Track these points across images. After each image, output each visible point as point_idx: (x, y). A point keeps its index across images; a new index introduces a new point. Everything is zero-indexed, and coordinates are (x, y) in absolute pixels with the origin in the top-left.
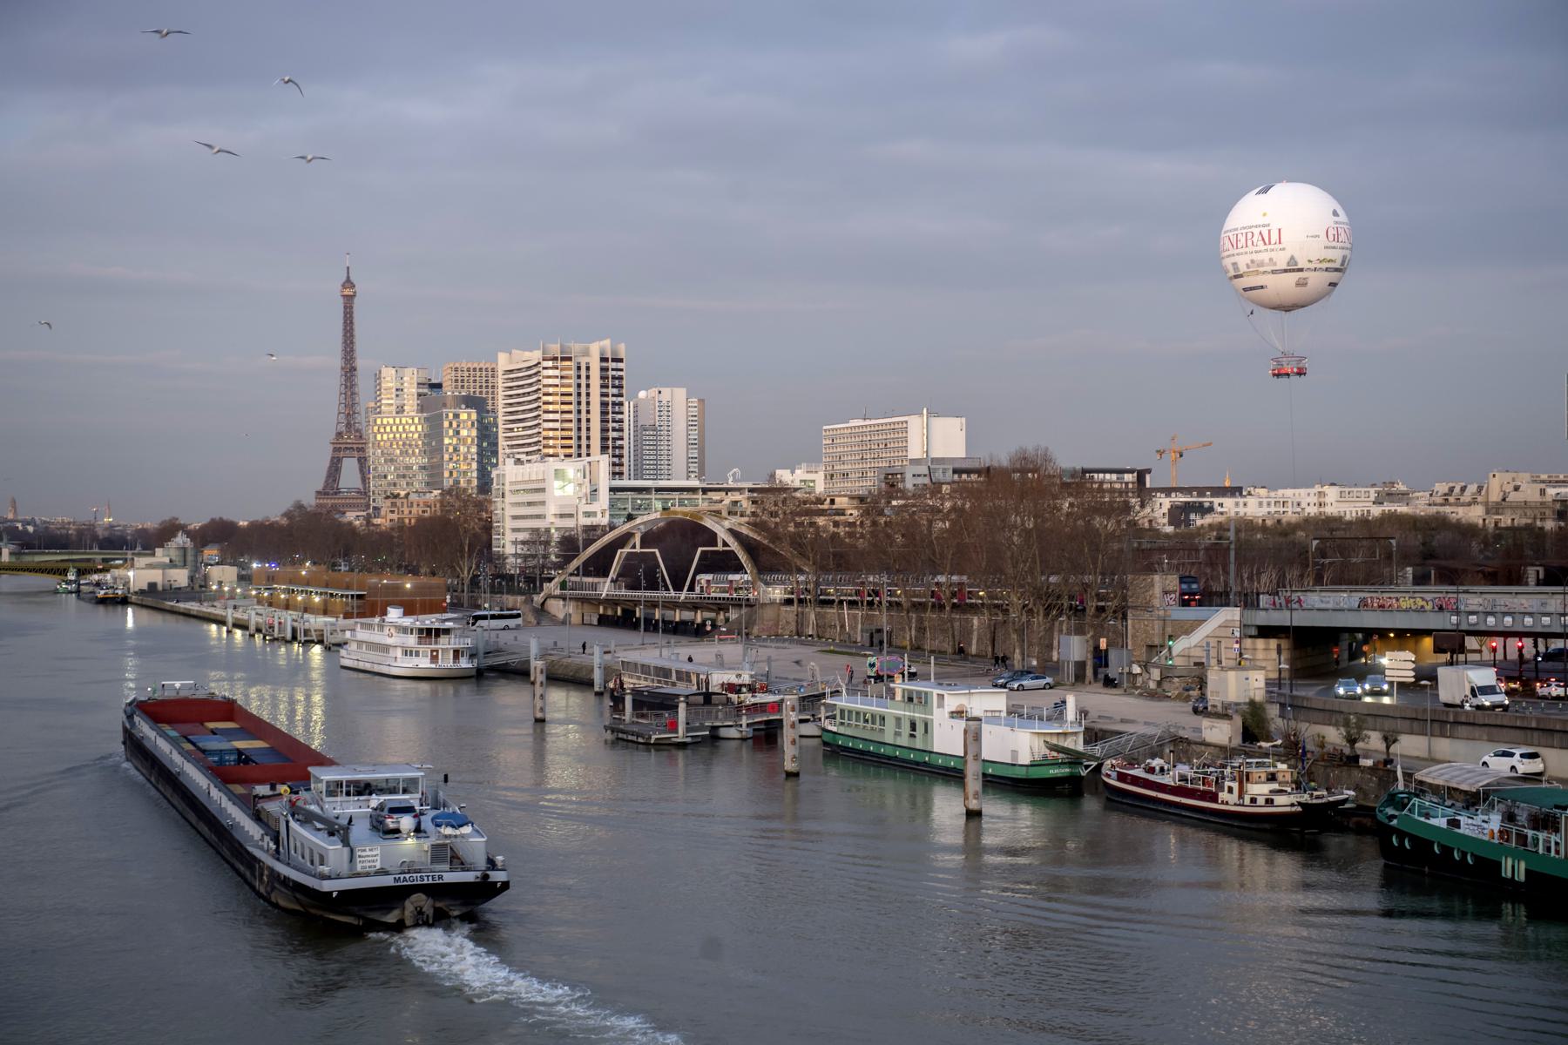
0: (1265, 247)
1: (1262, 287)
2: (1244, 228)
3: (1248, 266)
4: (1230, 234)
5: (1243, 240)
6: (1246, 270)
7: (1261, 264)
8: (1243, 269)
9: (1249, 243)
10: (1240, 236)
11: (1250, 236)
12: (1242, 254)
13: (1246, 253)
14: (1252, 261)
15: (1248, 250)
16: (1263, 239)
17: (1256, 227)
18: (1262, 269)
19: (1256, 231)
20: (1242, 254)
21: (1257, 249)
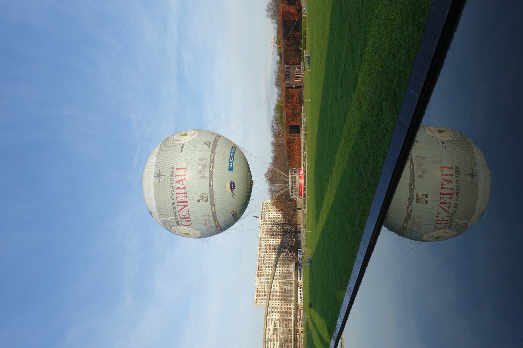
2: (172, 193)
5: (182, 196)
9: (183, 191)
10: (179, 200)
11: (179, 191)
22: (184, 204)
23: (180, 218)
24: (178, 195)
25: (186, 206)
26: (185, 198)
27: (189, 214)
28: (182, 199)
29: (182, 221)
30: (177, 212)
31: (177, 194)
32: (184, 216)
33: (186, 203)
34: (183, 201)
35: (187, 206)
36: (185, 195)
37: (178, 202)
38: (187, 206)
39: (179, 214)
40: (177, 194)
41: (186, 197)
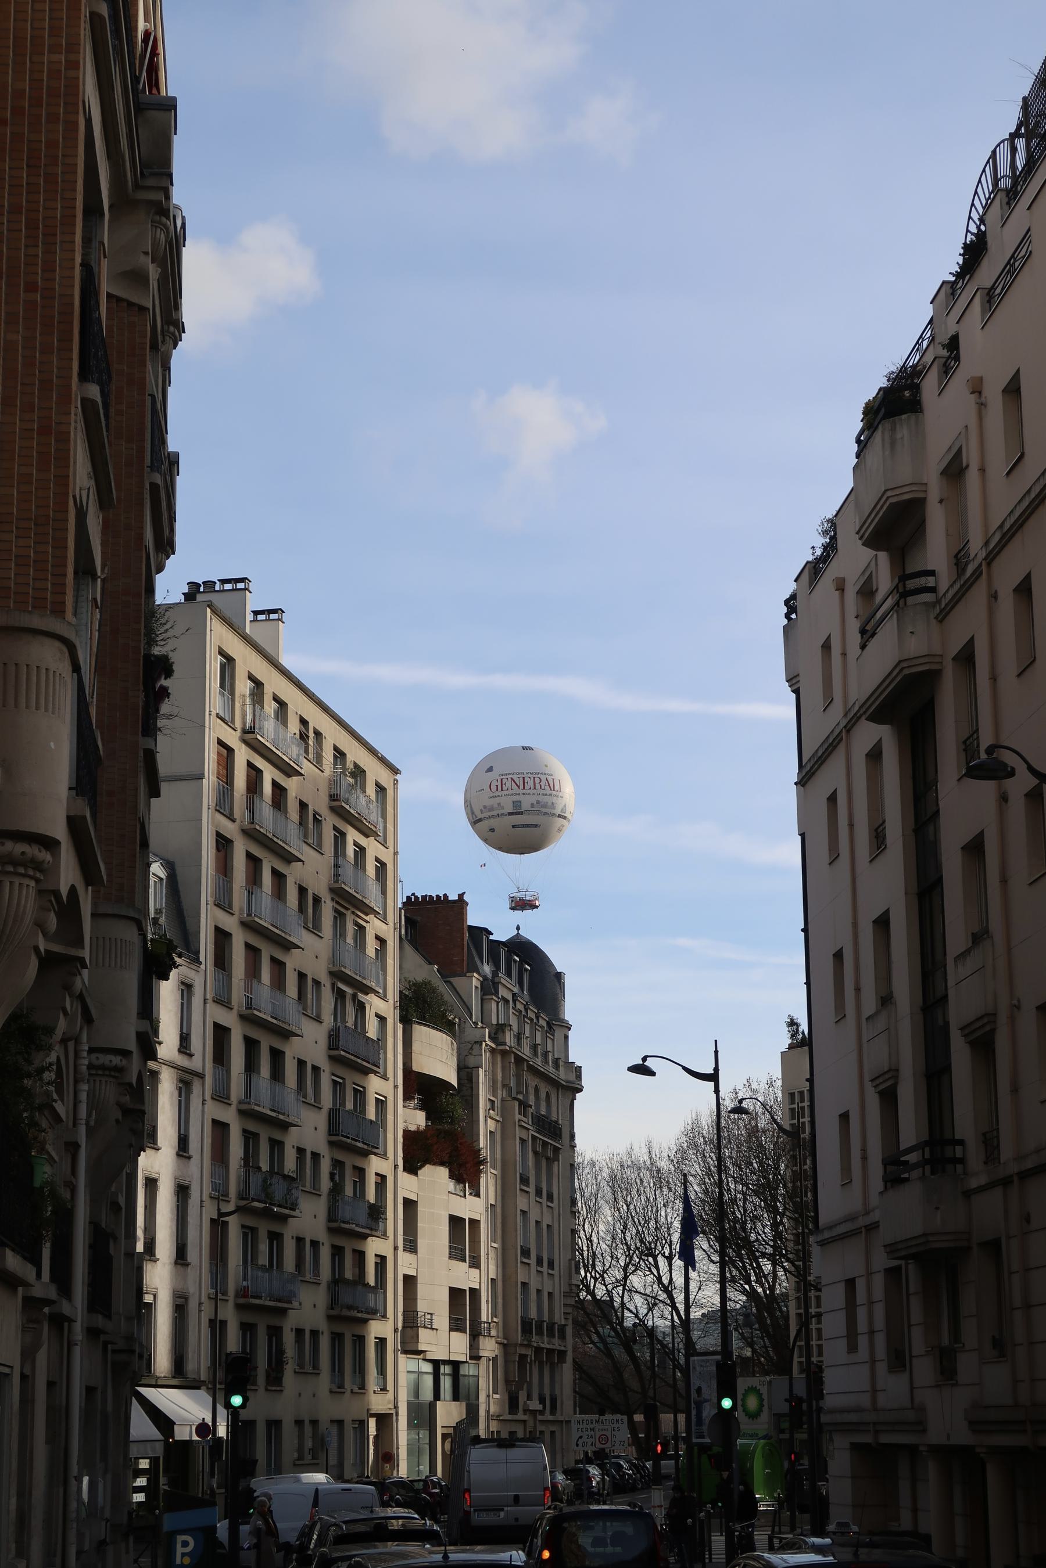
0: (550, 792)
1: (536, 826)
3: (532, 805)
4: (515, 777)
5: (531, 783)
7: (545, 806)
8: (526, 806)
9: (538, 786)
10: (526, 780)
11: (537, 780)
12: (529, 794)
13: (534, 794)
14: (538, 802)
15: (535, 791)
16: (549, 785)
17: (542, 774)
18: (544, 810)
19: (543, 778)
20: (529, 794)
22: (521, 787)
24: (532, 779)
25: (519, 787)
31: (534, 778)
34: (526, 784)
36: (533, 787)
37: (524, 778)
40: (534, 778)
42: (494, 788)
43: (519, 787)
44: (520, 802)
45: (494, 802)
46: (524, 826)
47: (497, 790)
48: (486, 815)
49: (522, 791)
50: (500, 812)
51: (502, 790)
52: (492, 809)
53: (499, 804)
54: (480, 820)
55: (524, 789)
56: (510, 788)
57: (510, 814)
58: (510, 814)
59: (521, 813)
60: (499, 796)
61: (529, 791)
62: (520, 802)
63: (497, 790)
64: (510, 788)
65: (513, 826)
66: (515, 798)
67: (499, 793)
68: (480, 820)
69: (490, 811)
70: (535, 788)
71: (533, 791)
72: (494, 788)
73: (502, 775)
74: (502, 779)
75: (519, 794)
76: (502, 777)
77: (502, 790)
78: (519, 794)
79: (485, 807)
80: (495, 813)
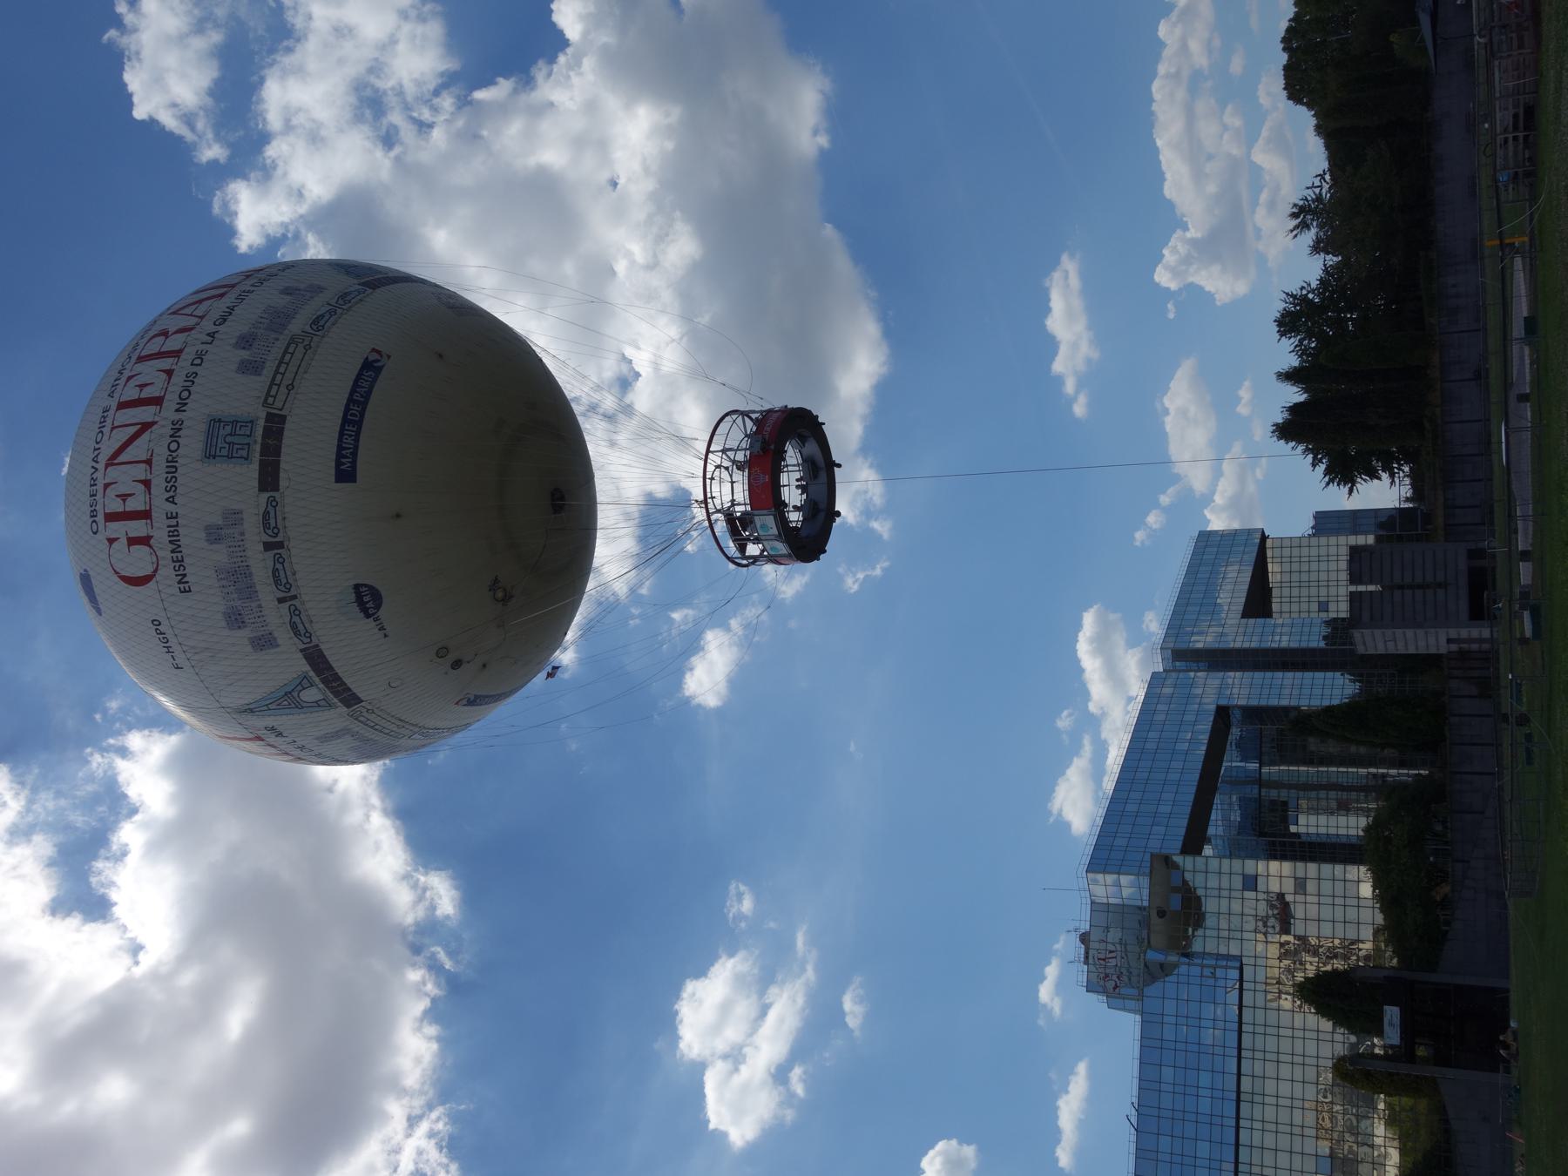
1: (370, 368)
3: (250, 368)
4: (107, 451)
6: (258, 384)
7: (277, 320)
9: (174, 343)
12: (191, 378)
14: (245, 341)
18: (297, 325)
20: (191, 378)
21: (215, 315)
22: (145, 414)
23: (111, 517)
24: (139, 368)
25: (146, 426)
26: (164, 376)
27: (147, 484)
28: (142, 386)
29: (111, 541)
30: (101, 466)
32: (124, 497)
33: (152, 409)
34: (147, 393)
35: (153, 423)
36: (166, 363)
37: (123, 405)
38: (153, 423)
39: (107, 486)
41: (169, 373)
42: (138, 562)
43: (146, 426)
44: (215, 422)
45: (204, 560)
46: (352, 421)
47: (145, 541)
48: (275, 618)
49: (168, 412)
50: (254, 537)
51: (145, 515)
52: (237, 578)
53: (214, 535)
54: (316, 659)
55: (157, 401)
56: (140, 471)
57: (269, 479)
58: (269, 479)
59: (275, 426)
60: (174, 534)
61: (178, 380)
62: (215, 422)
63: (145, 541)
64: (140, 471)
65: (345, 474)
66: (192, 442)
67: (160, 535)
68: (316, 659)
69: (249, 592)
70: (176, 354)
71: (183, 366)
72: (138, 562)
73: (93, 514)
74: (111, 517)
75: (177, 428)
76: (100, 518)
77: (145, 515)
78: (177, 428)
79: (235, 619)
80: (260, 564)
